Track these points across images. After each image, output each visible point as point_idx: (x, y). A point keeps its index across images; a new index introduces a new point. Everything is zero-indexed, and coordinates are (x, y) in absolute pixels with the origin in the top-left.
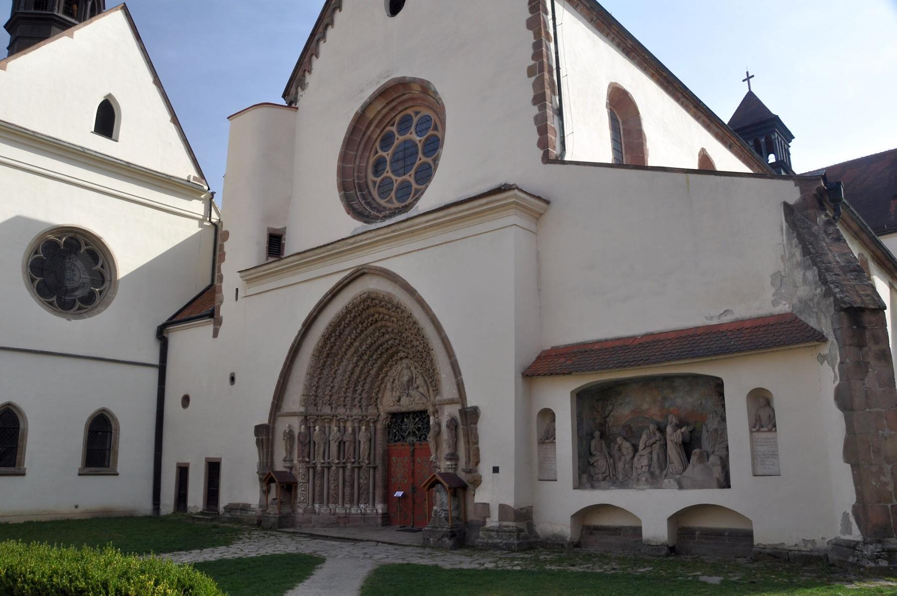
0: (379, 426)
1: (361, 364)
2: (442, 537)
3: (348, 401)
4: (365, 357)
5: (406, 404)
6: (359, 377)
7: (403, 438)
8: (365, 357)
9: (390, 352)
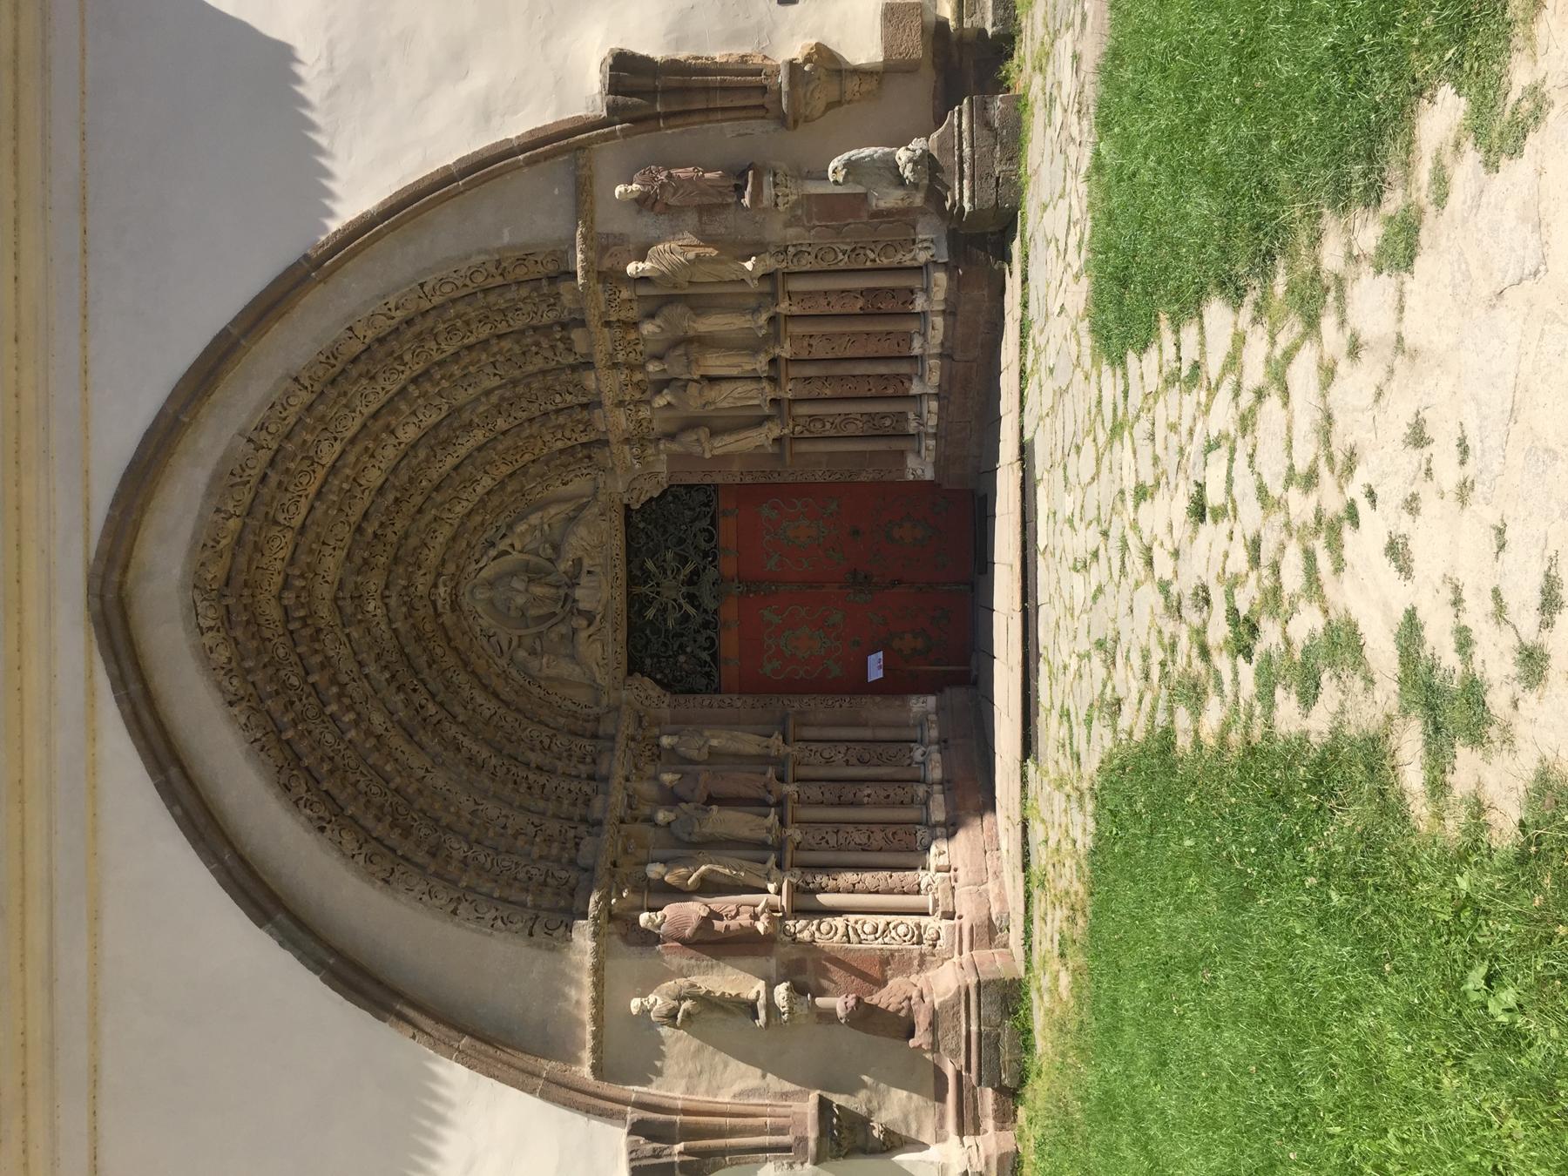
2: (988, 125)
5: (601, 592)
6: (499, 751)
7: (706, 625)
8: (432, 709)
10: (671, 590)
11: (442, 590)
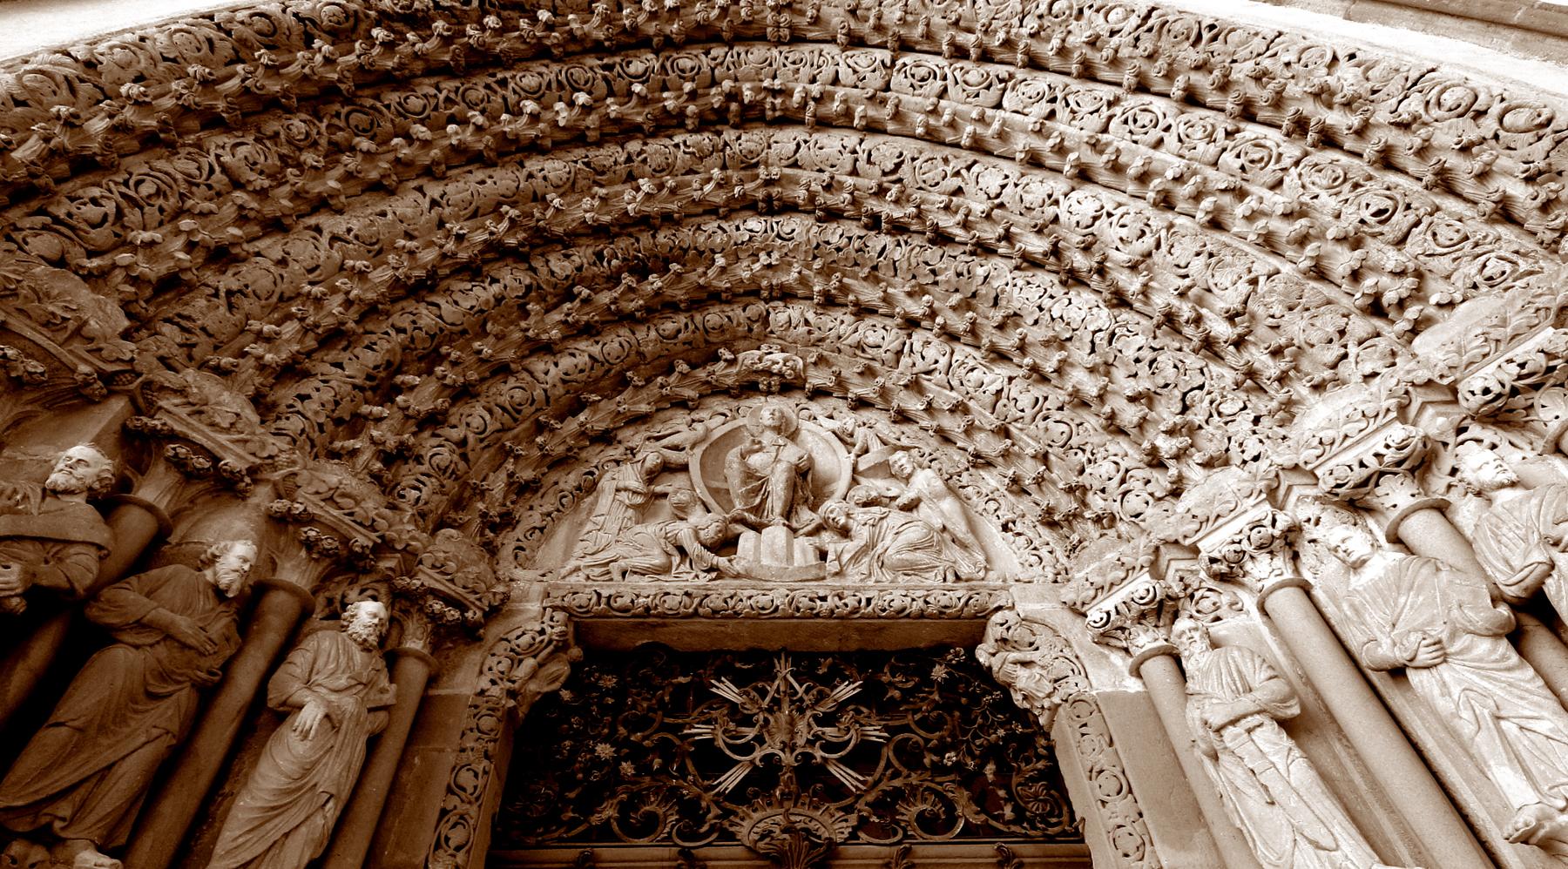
0: (474, 679)
1: (511, 279)
3: (334, 380)
4: (560, 266)
7: (691, 811)
8: (560, 266)
9: (714, 317)
10: (788, 735)
11: (778, 356)
